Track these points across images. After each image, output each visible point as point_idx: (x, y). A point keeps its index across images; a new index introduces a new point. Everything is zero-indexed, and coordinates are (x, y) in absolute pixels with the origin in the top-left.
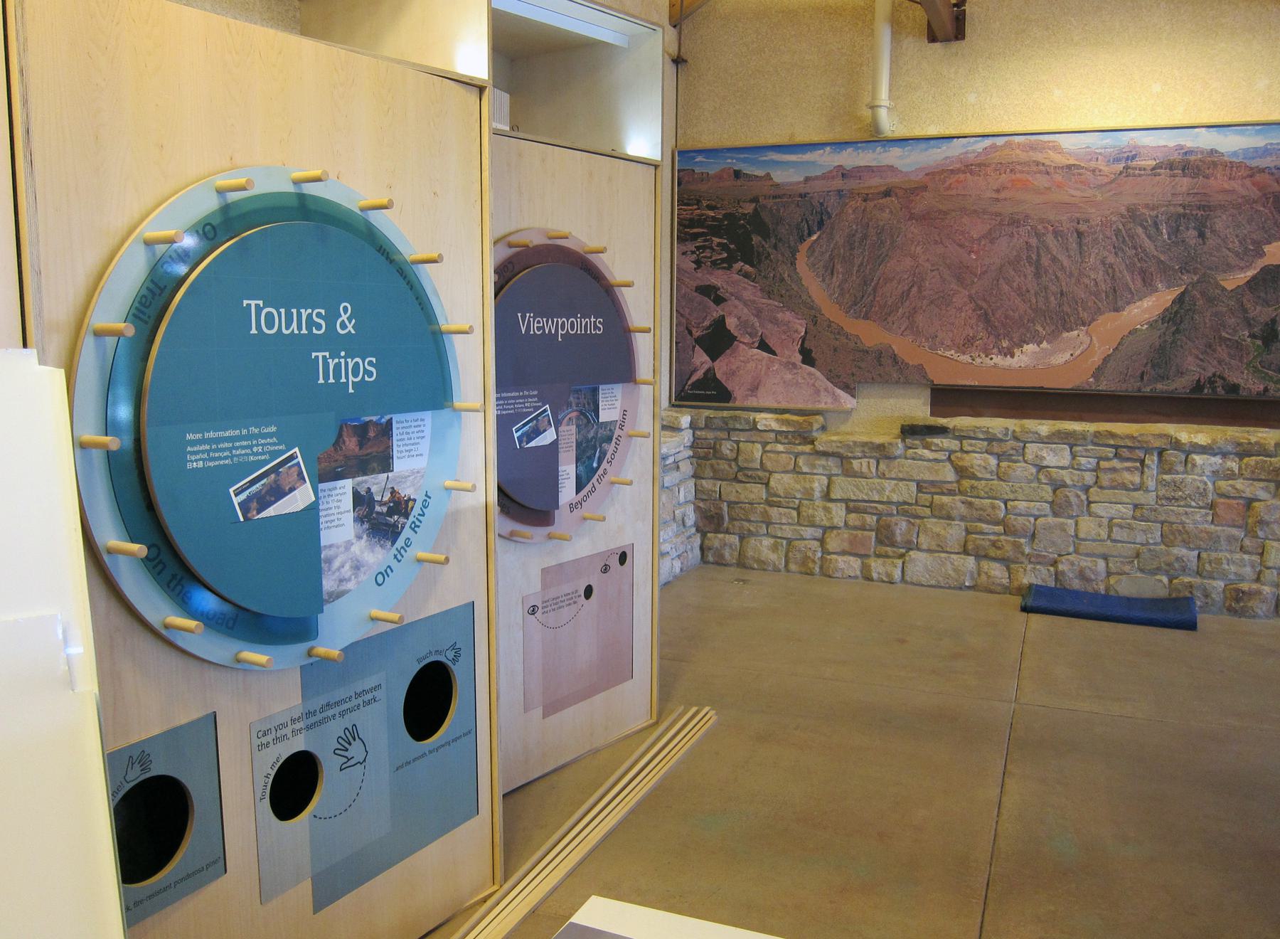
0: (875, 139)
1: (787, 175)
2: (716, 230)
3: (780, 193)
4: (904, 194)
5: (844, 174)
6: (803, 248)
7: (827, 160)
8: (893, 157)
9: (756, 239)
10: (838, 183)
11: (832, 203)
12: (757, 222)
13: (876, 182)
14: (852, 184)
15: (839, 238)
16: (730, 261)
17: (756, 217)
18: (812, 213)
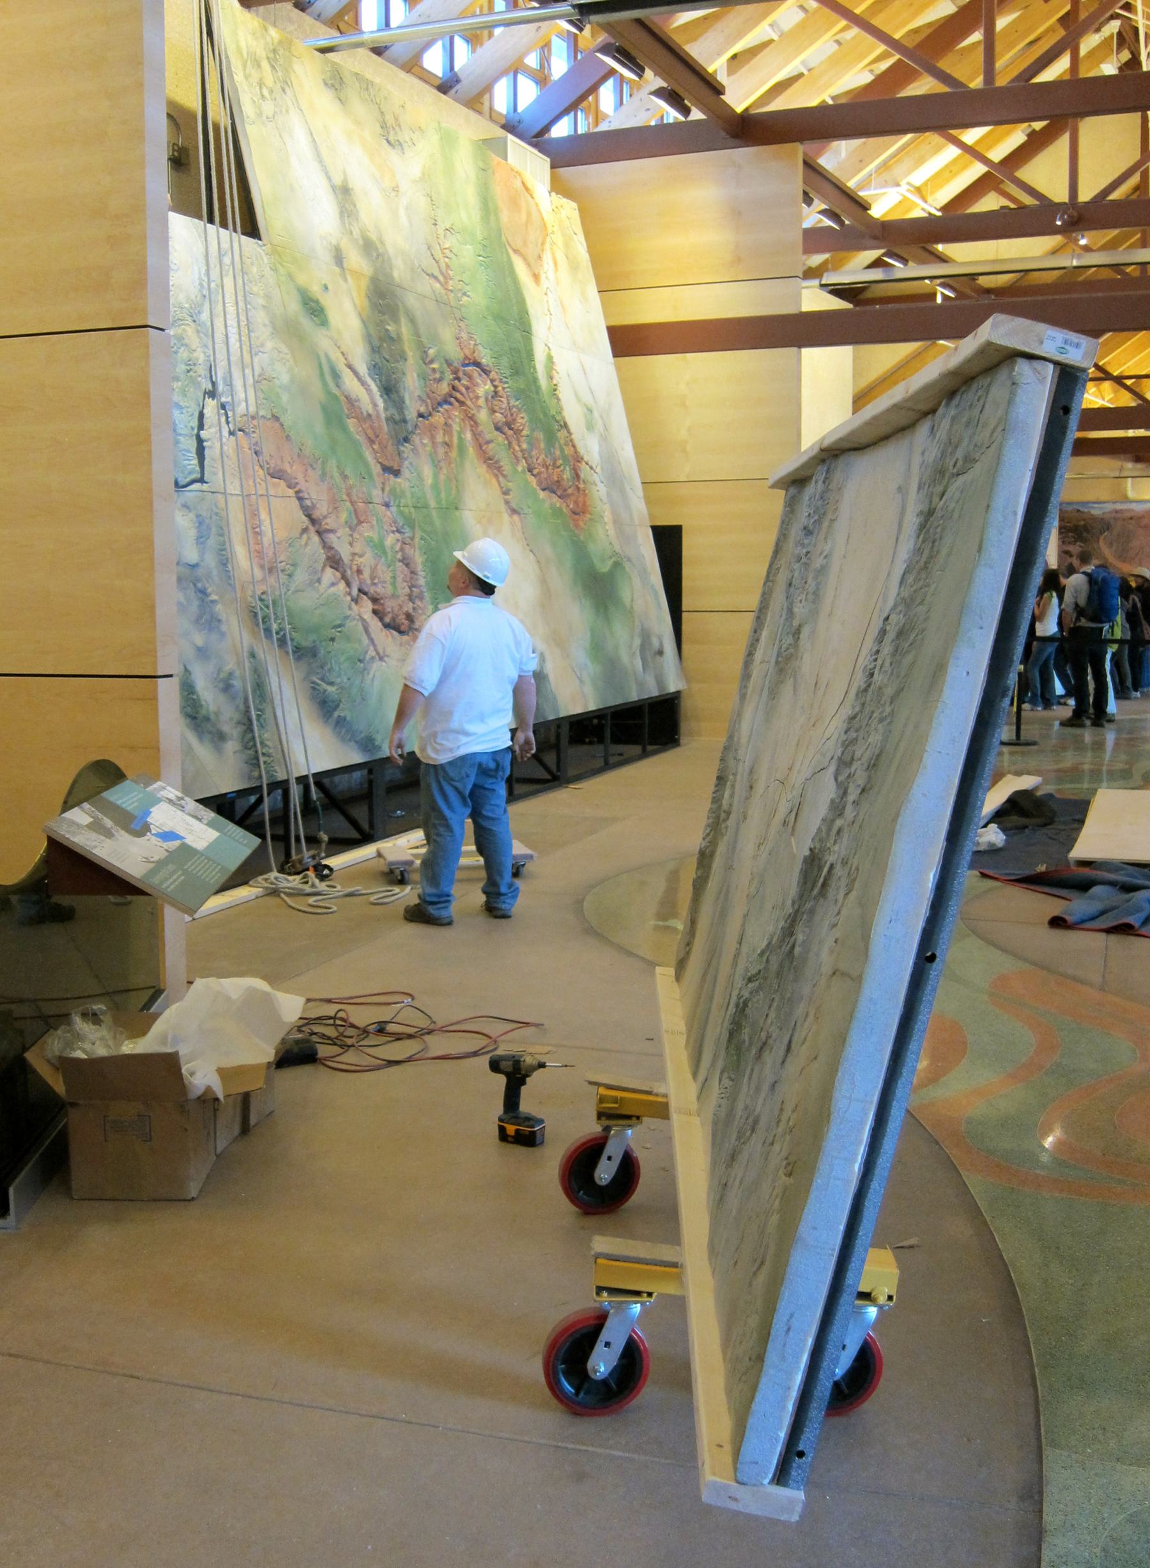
0: (1126, 499)
1: (1096, 512)
2: (1070, 530)
3: (1094, 519)
4: (1135, 519)
5: (1117, 512)
6: (1102, 538)
7: (1109, 507)
8: (1134, 506)
9: (1085, 534)
10: (1114, 515)
11: (1112, 522)
12: (1086, 528)
13: (1128, 515)
14: (1119, 515)
15: (1115, 533)
16: (1075, 542)
17: (1085, 526)
18: (1105, 525)
